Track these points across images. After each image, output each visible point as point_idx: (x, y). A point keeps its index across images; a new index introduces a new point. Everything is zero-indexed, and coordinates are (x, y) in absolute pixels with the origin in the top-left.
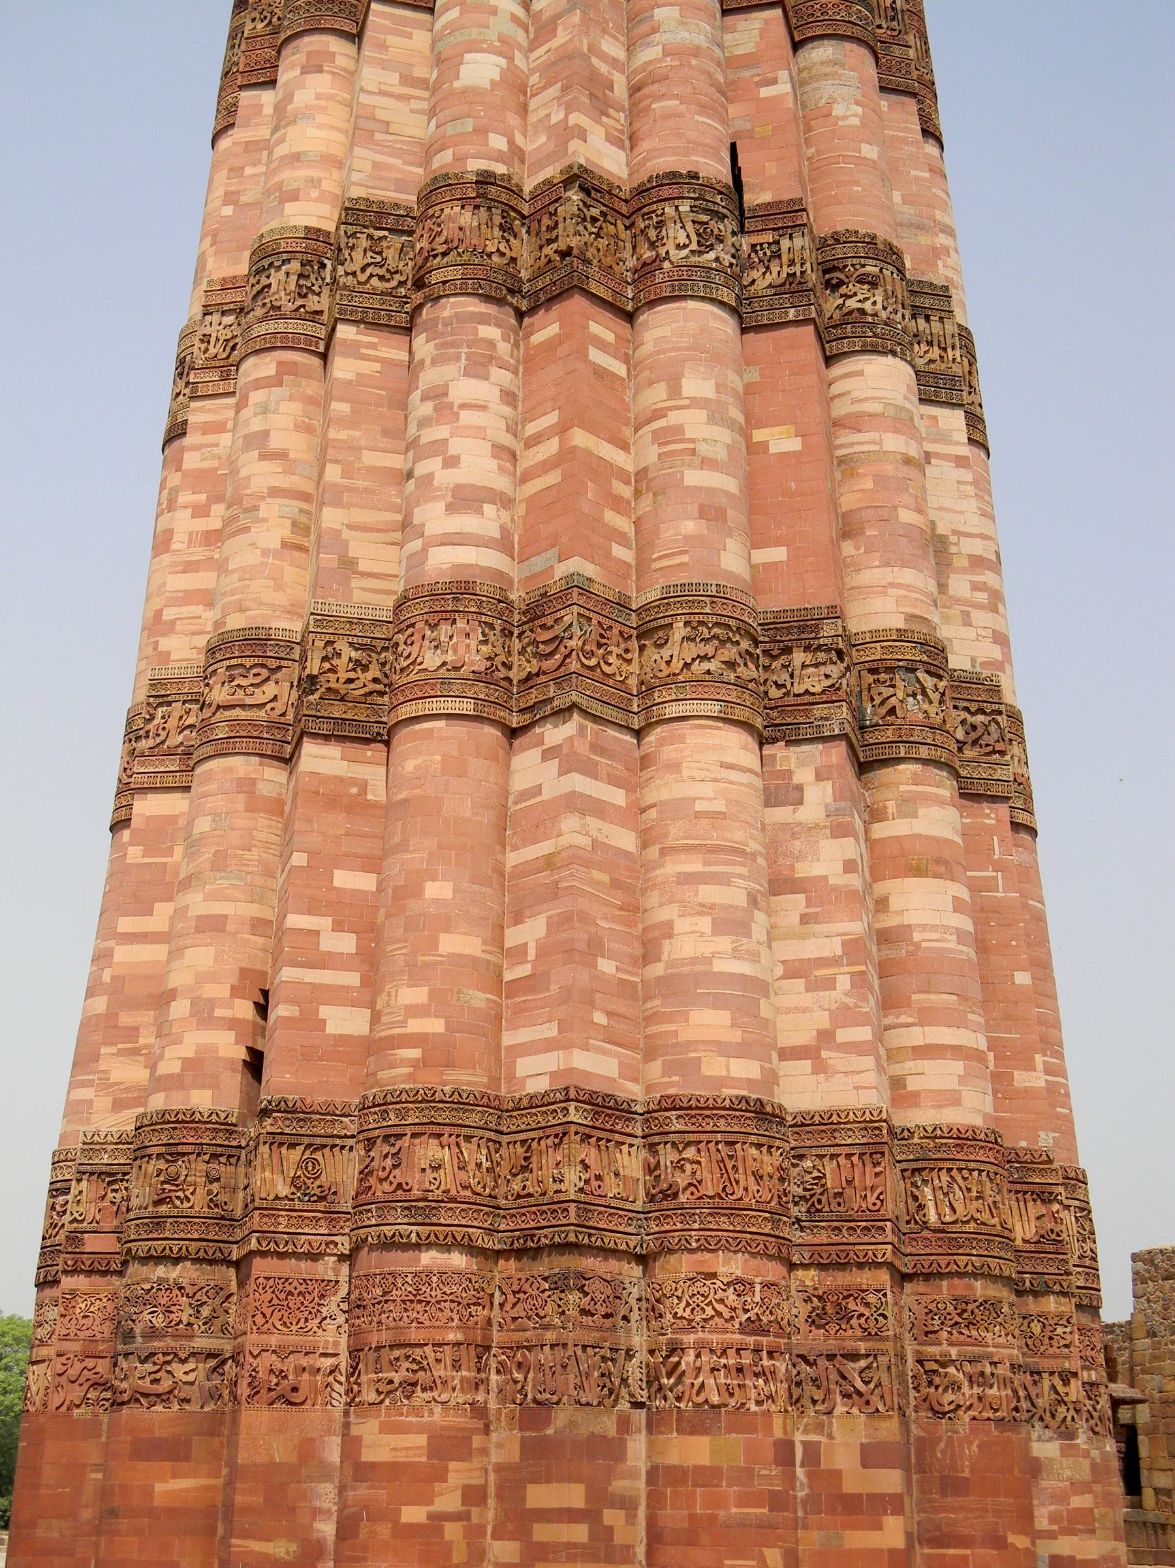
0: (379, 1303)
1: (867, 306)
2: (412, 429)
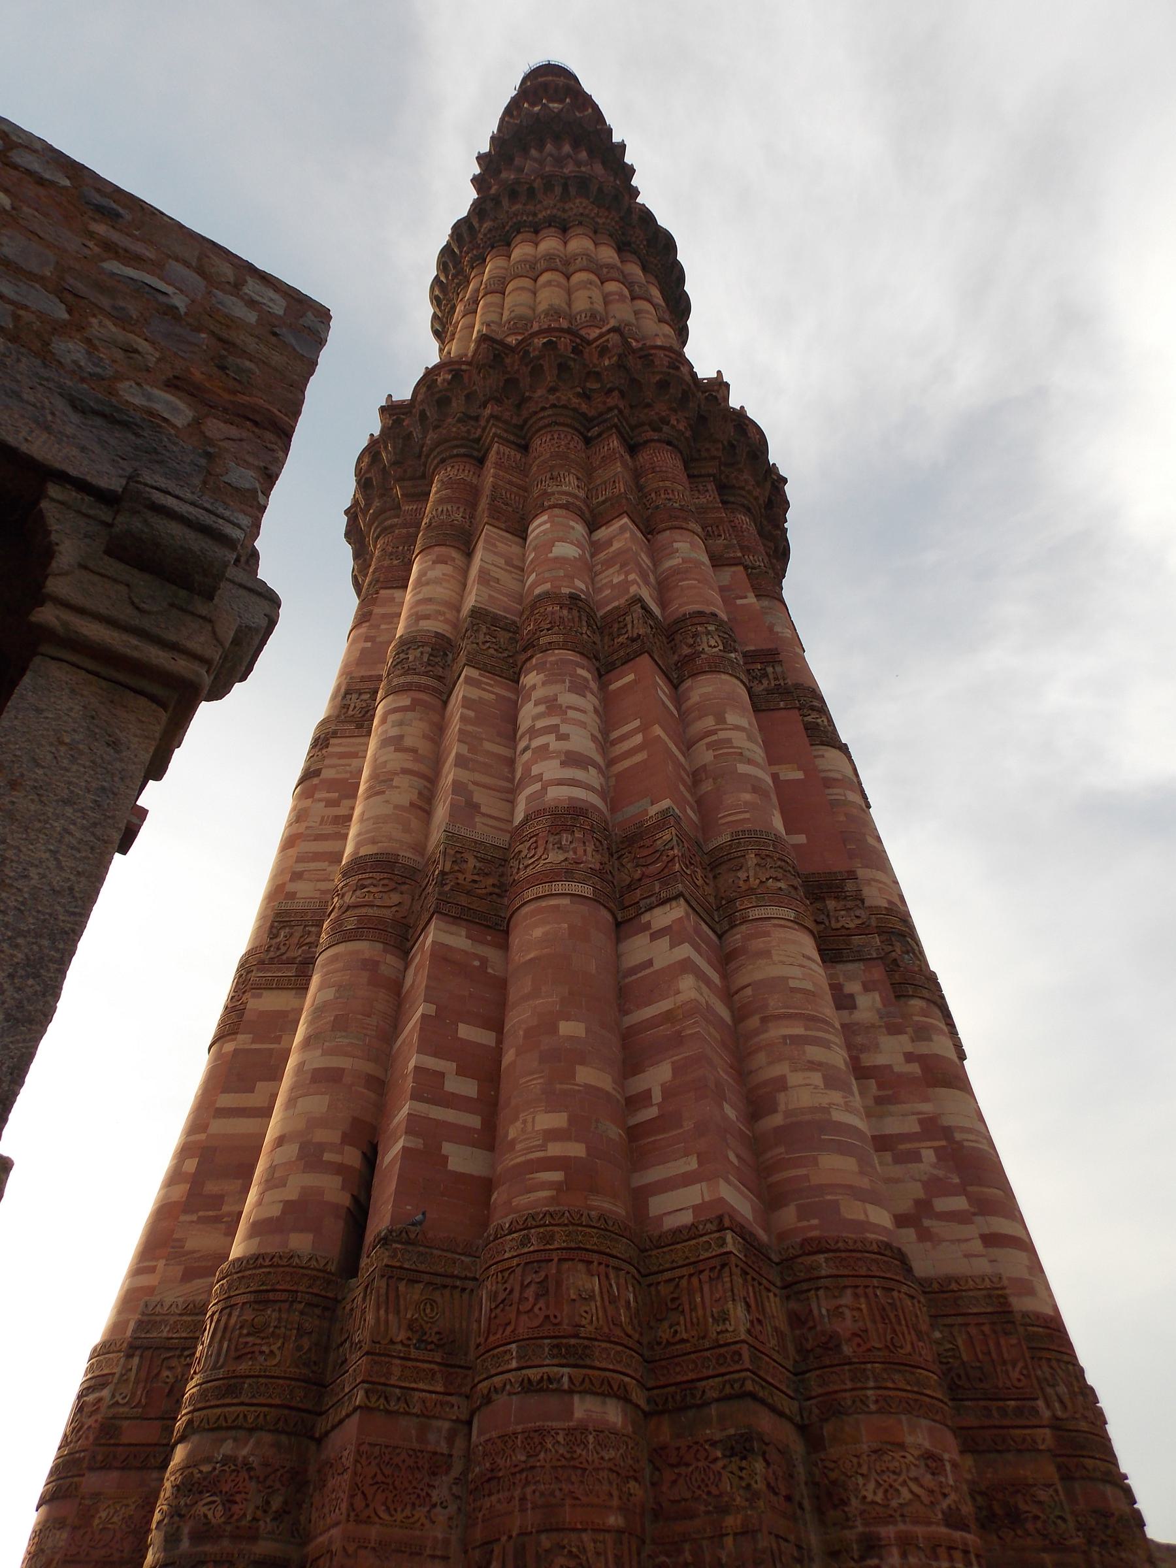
0: (521, 1471)
2: (524, 722)
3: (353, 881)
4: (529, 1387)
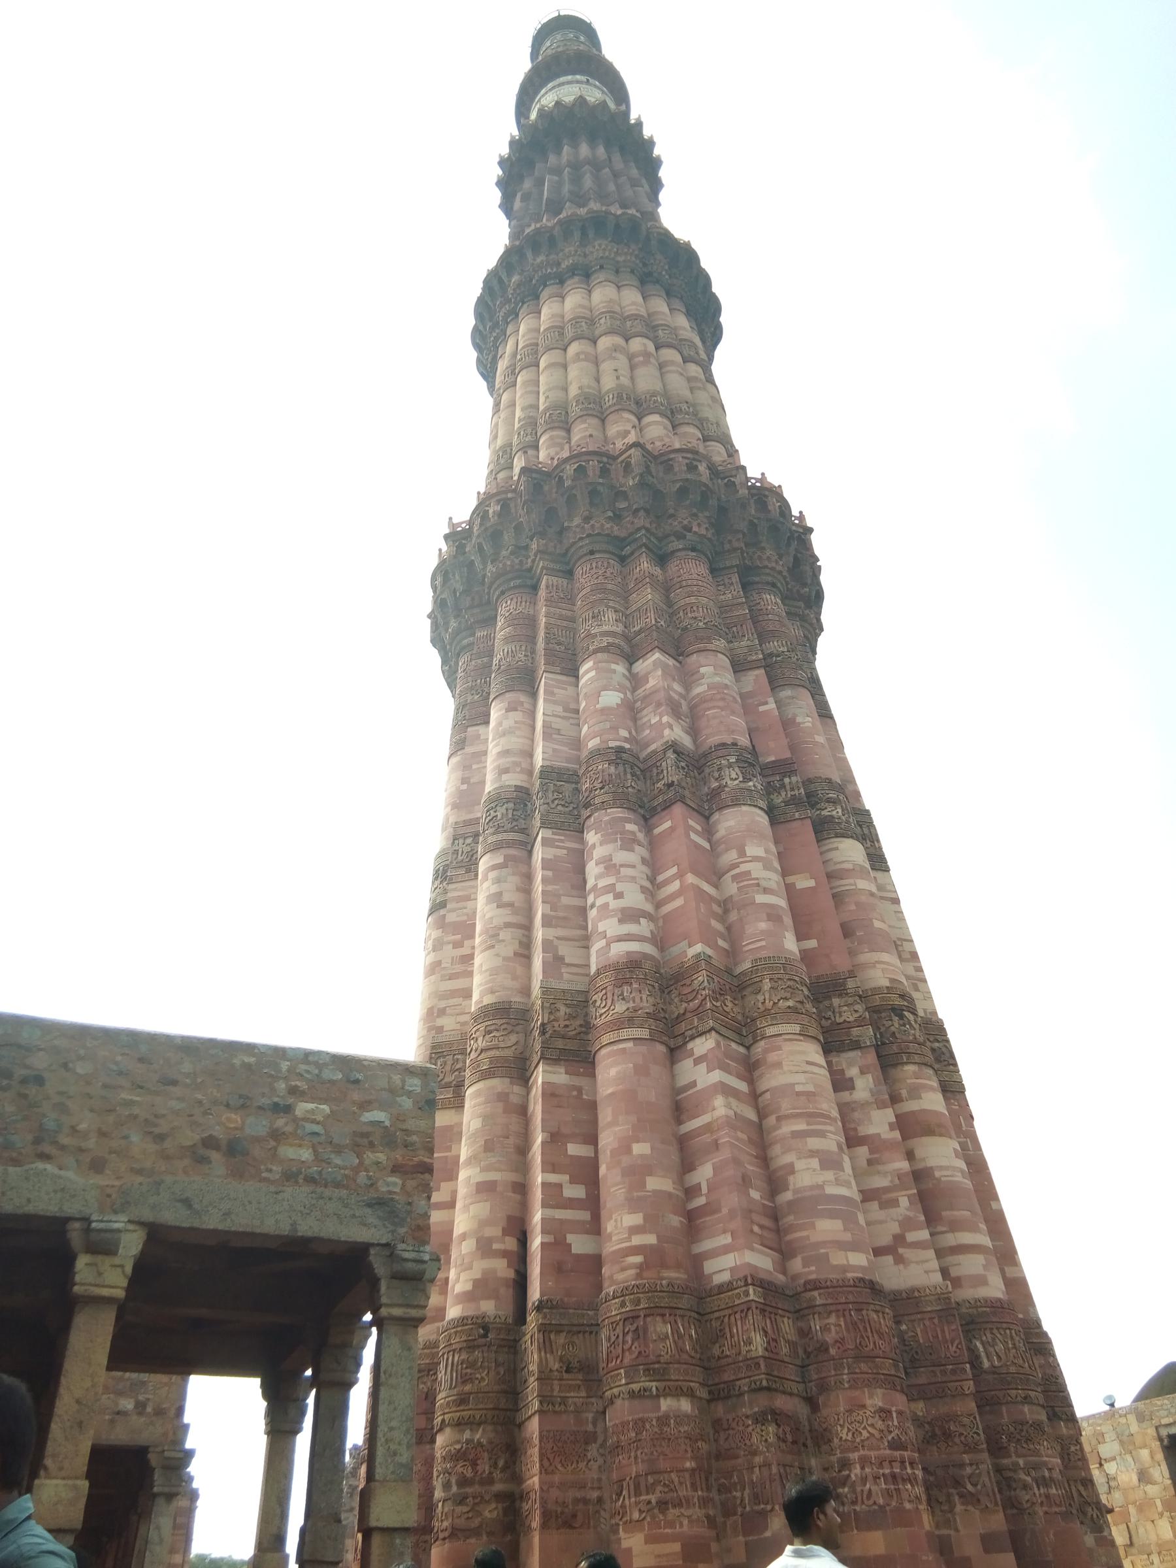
1: (834, 813)
2: (590, 884)
3: (482, 1027)
4: (633, 1395)
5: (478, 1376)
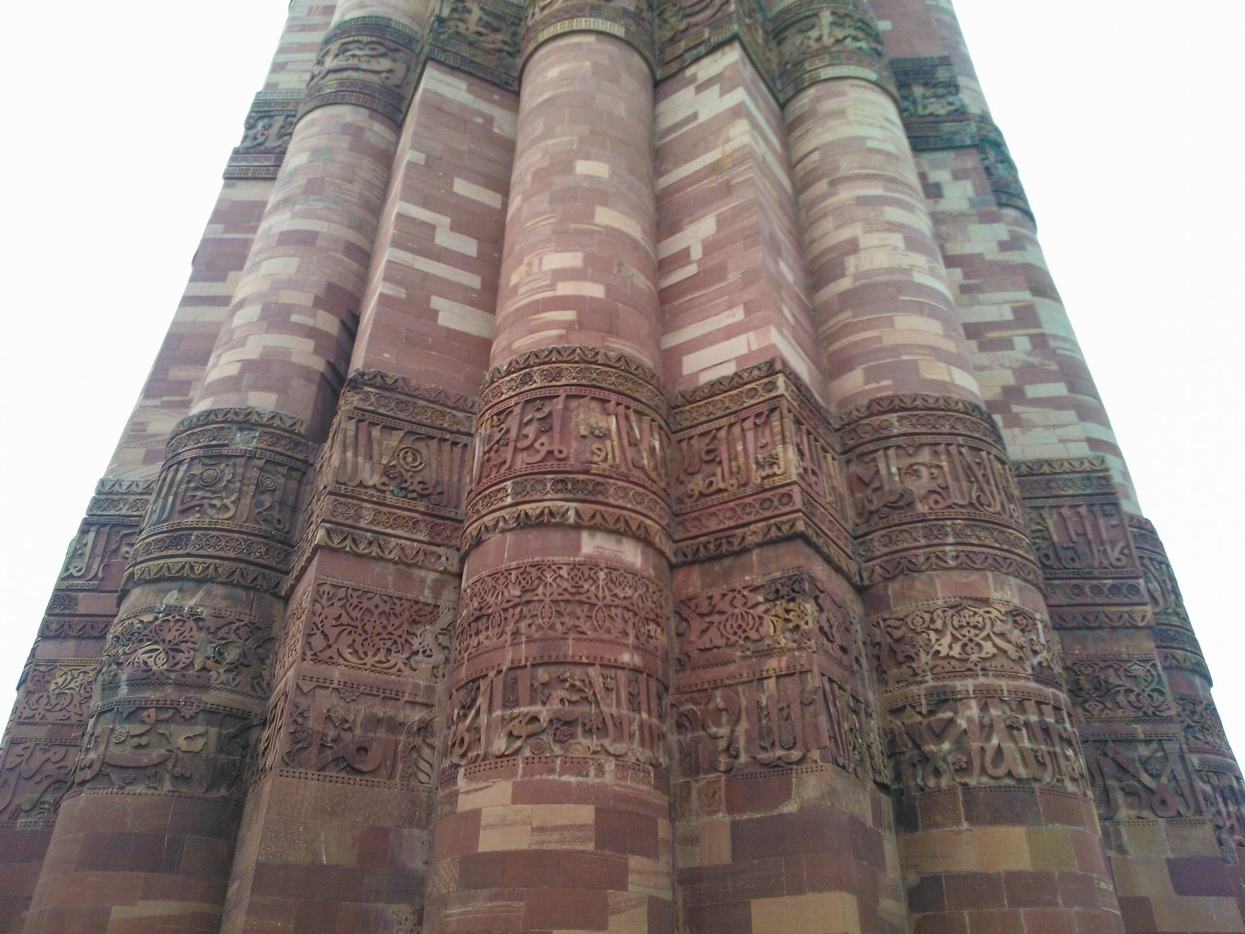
3: (334, 47)
4: (525, 523)
5: (217, 502)
